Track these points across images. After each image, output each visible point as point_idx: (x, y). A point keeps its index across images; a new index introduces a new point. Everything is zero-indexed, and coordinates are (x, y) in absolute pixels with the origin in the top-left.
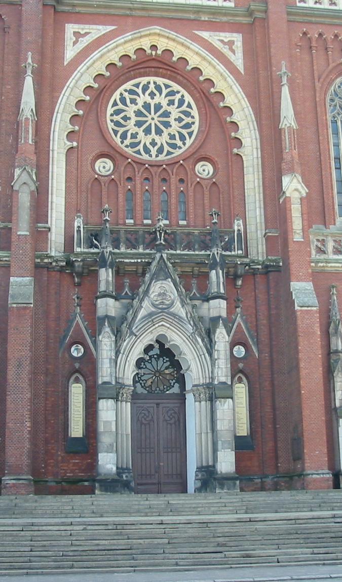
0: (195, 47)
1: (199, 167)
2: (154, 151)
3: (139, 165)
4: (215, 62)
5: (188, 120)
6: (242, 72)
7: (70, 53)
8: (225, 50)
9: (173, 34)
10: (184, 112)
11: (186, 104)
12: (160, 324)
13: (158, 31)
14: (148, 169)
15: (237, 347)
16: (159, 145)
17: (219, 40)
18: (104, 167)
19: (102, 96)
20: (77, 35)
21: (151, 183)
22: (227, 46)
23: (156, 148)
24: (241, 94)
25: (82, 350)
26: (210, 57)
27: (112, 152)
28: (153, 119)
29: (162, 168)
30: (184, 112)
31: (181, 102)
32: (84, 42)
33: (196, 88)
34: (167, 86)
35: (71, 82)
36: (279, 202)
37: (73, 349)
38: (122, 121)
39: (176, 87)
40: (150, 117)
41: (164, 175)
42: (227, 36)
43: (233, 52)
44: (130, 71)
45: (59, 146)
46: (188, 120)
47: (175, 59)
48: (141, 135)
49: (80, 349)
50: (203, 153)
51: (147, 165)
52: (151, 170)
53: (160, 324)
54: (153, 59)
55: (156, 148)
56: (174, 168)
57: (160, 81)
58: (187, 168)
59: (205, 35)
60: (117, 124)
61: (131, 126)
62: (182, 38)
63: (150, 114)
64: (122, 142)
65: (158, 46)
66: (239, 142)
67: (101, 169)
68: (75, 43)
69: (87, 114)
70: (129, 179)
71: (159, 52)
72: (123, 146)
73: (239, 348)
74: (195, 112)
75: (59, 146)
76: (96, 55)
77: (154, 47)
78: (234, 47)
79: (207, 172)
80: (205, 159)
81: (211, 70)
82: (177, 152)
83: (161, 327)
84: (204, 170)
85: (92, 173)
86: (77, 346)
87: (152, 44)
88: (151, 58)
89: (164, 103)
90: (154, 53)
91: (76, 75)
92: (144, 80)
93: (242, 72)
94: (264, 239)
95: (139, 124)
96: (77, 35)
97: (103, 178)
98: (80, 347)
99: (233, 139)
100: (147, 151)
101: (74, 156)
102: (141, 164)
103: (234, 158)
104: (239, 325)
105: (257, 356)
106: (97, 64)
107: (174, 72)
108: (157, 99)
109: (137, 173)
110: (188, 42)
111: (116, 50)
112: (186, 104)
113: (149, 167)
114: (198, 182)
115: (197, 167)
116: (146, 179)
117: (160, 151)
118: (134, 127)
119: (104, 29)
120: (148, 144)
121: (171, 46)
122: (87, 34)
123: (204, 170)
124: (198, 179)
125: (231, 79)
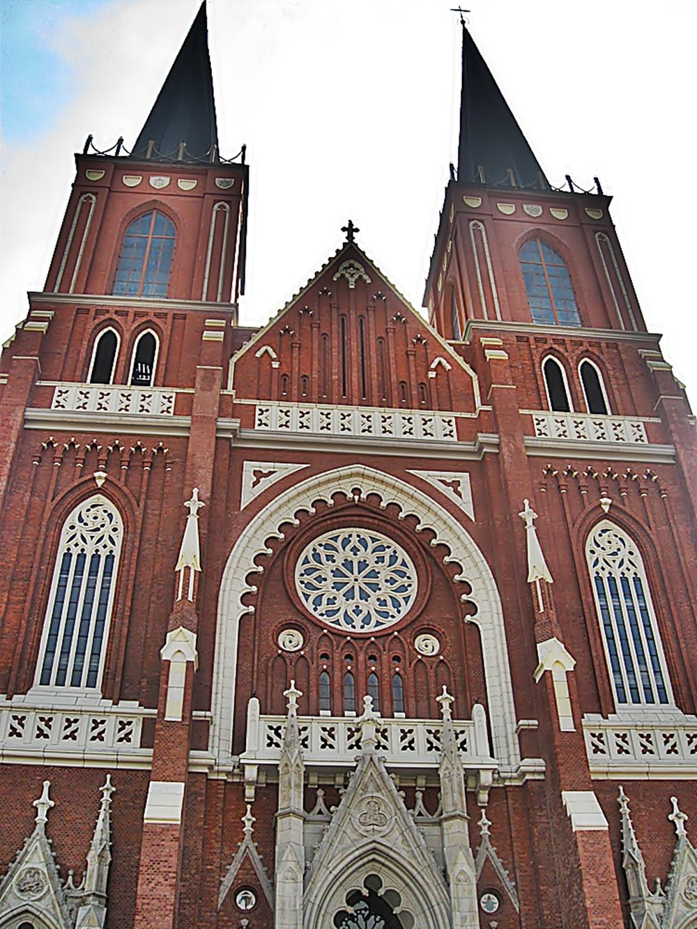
0: (409, 489)
1: (419, 642)
2: (358, 621)
3: (337, 638)
4: (436, 507)
5: (401, 581)
7: (248, 495)
8: (449, 492)
9: (380, 475)
11: (399, 561)
12: (370, 857)
14: (352, 643)
15: (486, 896)
16: (365, 612)
17: (439, 480)
18: (291, 640)
19: (288, 551)
20: (259, 474)
21: (354, 661)
23: (361, 616)
25: (254, 900)
26: (429, 501)
28: (356, 580)
29: (369, 642)
31: (393, 559)
32: (265, 484)
33: (413, 541)
34: (374, 540)
35: (249, 530)
36: (535, 680)
37: (239, 898)
39: (386, 540)
40: (352, 578)
42: (449, 476)
44: (326, 520)
46: (401, 581)
47: (383, 504)
48: (341, 600)
49: (250, 898)
51: (349, 638)
52: (355, 644)
53: (370, 857)
54: (357, 506)
55: (361, 616)
56: (385, 642)
57: (365, 533)
58: (404, 642)
60: (309, 586)
61: (327, 588)
62: (390, 479)
63: (352, 573)
64: (315, 609)
65: (362, 489)
67: (287, 643)
68: (255, 484)
70: (325, 656)
71: (363, 496)
72: (316, 614)
73: (489, 897)
74: (411, 571)
76: (282, 498)
77: (356, 491)
78: (459, 489)
79: (430, 648)
80: (430, 631)
81: (431, 517)
82: (389, 623)
83: (370, 864)
84: (428, 645)
85: (275, 647)
86: (246, 893)
87: (355, 486)
88: (353, 503)
89: (371, 559)
90: (356, 498)
91: (256, 522)
92: (343, 533)
94: (516, 735)
95: (337, 586)
96: (259, 474)
97: (288, 654)
98: (251, 894)
99: (463, 604)
100: (349, 620)
102: (342, 635)
103: (467, 628)
105: (518, 909)
106: (283, 510)
107: (384, 521)
108: (362, 554)
109: (335, 648)
110: (400, 484)
111: (309, 494)
112: (399, 561)
113: (352, 641)
114: (420, 660)
115: (416, 640)
116: (348, 656)
117: (367, 620)
118: (331, 589)
120: (350, 612)
121: (379, 489)
123: (426, 646)
124: (419, 657)
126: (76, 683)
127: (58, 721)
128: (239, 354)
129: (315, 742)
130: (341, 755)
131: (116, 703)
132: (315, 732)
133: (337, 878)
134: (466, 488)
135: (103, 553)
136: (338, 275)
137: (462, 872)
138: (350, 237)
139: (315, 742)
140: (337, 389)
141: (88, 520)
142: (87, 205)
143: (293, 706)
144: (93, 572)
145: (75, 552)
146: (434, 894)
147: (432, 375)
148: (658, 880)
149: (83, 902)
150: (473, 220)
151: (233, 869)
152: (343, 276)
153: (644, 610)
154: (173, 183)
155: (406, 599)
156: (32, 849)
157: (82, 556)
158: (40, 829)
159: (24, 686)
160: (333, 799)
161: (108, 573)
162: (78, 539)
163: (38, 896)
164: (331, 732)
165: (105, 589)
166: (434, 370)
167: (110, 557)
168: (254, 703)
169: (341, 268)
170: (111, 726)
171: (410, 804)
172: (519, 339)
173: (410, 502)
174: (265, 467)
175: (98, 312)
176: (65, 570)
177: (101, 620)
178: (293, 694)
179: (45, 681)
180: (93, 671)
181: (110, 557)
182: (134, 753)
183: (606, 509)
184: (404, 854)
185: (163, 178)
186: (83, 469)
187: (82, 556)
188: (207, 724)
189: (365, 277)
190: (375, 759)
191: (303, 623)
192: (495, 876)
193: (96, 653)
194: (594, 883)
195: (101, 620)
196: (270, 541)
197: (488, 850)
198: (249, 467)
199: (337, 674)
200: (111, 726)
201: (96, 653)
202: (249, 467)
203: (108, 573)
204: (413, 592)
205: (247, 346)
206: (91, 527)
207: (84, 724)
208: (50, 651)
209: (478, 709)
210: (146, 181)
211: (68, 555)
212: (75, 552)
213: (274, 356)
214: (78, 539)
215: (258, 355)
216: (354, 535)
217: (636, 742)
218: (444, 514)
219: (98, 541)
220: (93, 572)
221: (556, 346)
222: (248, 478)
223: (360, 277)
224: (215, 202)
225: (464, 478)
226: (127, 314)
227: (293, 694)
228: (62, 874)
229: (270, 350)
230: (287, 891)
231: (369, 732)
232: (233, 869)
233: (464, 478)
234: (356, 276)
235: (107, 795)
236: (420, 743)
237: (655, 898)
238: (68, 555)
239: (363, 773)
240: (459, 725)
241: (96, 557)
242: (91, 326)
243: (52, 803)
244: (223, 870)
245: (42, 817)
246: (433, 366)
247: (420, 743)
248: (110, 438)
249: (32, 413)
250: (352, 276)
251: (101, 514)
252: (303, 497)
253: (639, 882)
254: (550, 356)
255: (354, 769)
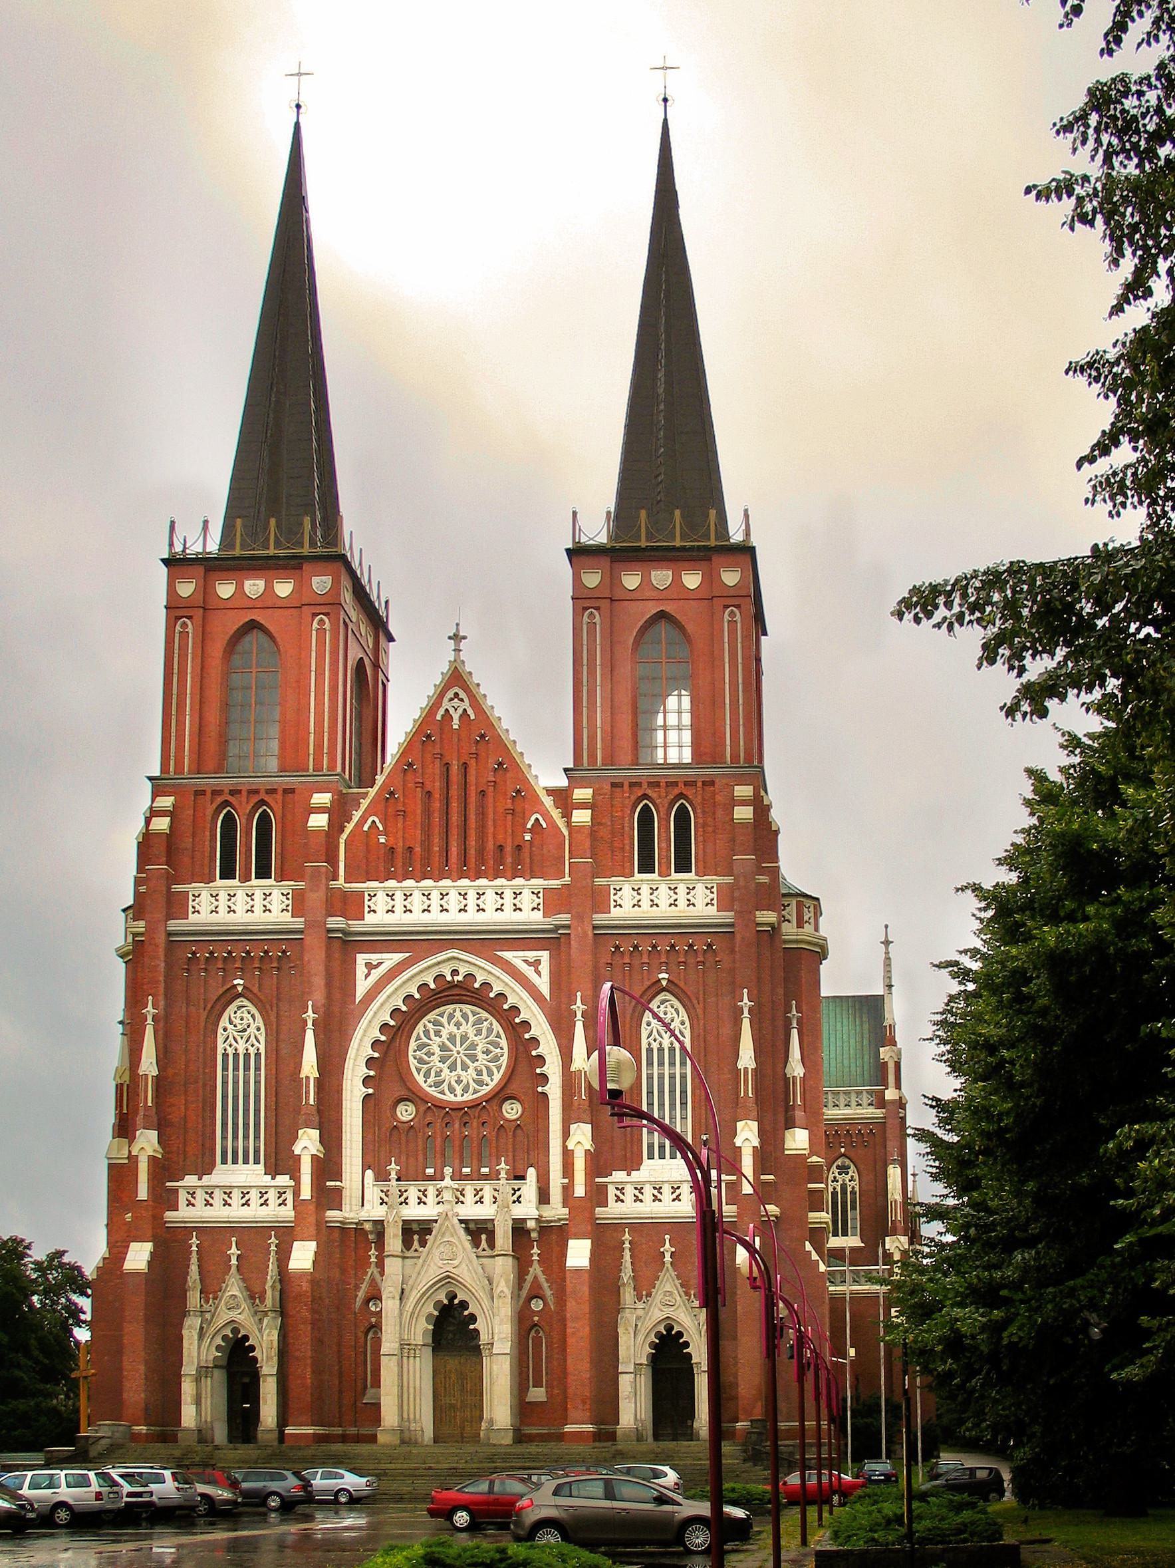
0: (497, 971)
1: (506, 1106)
6: (548, 999)
7: (362, 986)
8: (529, 972)
10: (491, 1043)
13: (456, 955)
22: (532, 968)
24: (546, 1026)
27: (412, 1096)
30: (491, 1043)
31: (490, 1031)
32: (376, 974)
35: (364, 1023)
38: (425, 1057)
41: (466, 1119)
42: (531, 955)
43: (539, 974)
45: (353, 1092)
50: (509, 1091)
57: (466, 1008)
59: (508, 955)
66: (544, 1078)
68: (367, 976)
69: (385, 1055)
75: (353, 1092)
76: (390, 989)
79: (515, 1111)
81: (517, 996)
91: (369, 1014)
93: (548, 999)
95: (443, 1060)
96: (370, 966)
101: (371, 1104)
103: (540, 1096)
104: (536, 1277)
106: (392, 998)
110: (488, 966)
119: (398, 957)
122: (380, 964)
125: (535, 1007)
126: (246, 1162)
127: (236, 1194)
128: (347, 831)
129: (413, 1200)
130: (427, 1212)
131: (273, 1178)
132: (413, 1193)
133: (424, 1294)
134: (545, 968)
135: (252, 1051)
136: (441, 712)
137: (502, 1291)
138: (457, 650)
139: (413, 1200)
140: (436, 859)
141: (237, 1021)
142: (184, 635)
143: (393, 1175)
144: (247, 1068)
145: (230, 1051)
146: (486, 1302)
147: (528, 838)
148: (644, 1293)
149: (265, 1313)
150: (589, 608)
151: (364, 1286)
152: (447, 710)
153: (683, 1077)
154: (269, 588)
155: (499, 1068)
156: (230, 1283)
157: (236, 1055)
158: (233, 1269)
159: (208, 1169)
160: (423, 1243)
161: (257, 1069)
162: (231, 1039)
163: (239, 1311)
164: (424, 1193)
165: (257, 1082)
166: (531, 831)
167: (258, 1055)
168: (369, 1173)
169: (446, 700)
170: (272, 1195)
171: (476, 1243)
172: (614, 785)
173: (500, 982)
174: (374, 958)
175: (216, 793)
176: (225, 1068)
177: (257, 1097)
178: (393, 1168)
179: (224, 1162)
180: (257, 1151)
181: (258, 1055)
182: (288, 1212)
183: (664, 983)
184: (467, 1278)
185: (257, 582)
186: (224, 977)
187: (236, 1055)
188: (339, 1191)
189: (470, 712)
190: (450, 1214)
191: (413, 1095)
192: (540, 1287)
193: (257, 1137)
194: (574, 1303)
195: (257, 1097)
196: (376, 1044)
197: (536, 1270)
198: (361, 959)
199: (439, 1140)
200: (272, 1195)
201: (257, 1137)
202: (361, 959)
203: (257, 1069)
204: (504, 1060)
205: (357, 815)
206: (239, 1027)
207: (254, 1195)
208: (224, 1138)
209: (531, 1173)
210: (240, 587)
211: (225, 1055)
212: (230, 1051)
213: (381, 829)
214: (231, 1039)
215: (366, 828)
216: (458, 1010)
217: (648, 1191)
218: (525, 995)
219: (247, 1041)
220: (247, 1068)
221: (649, 792)
222: (361, 970)
223: (465, 710)
224: (315, 615)
225: (545, 956)
226: (240, 792)
227: (393, 1168)
228: (252, 1297)
229: (377, 821)
230: (389, 1305)
231: (447, 1196)
232: (364, 1286)
233: (545, 956)
234: (460, 711)
235: (273, 1248)
236: (488, 1199)
237: (640, 1305)
238: (225, 1055)
239: (441, 1225)
240: (517, 1183)
241: (247, 1055)
242: (210, 810)
243: (239, 1252)
244: (357, 1288)
245: (234, 1262)
246: (529, 826)
247: (488, 1199)
248: (241, 944)
249: (174, 925)
250: (456, 710)
251: (246, 1015)
252: (409, 984)
253: (628, 1295)
254: (645, 801)
255: (436, 1221)
